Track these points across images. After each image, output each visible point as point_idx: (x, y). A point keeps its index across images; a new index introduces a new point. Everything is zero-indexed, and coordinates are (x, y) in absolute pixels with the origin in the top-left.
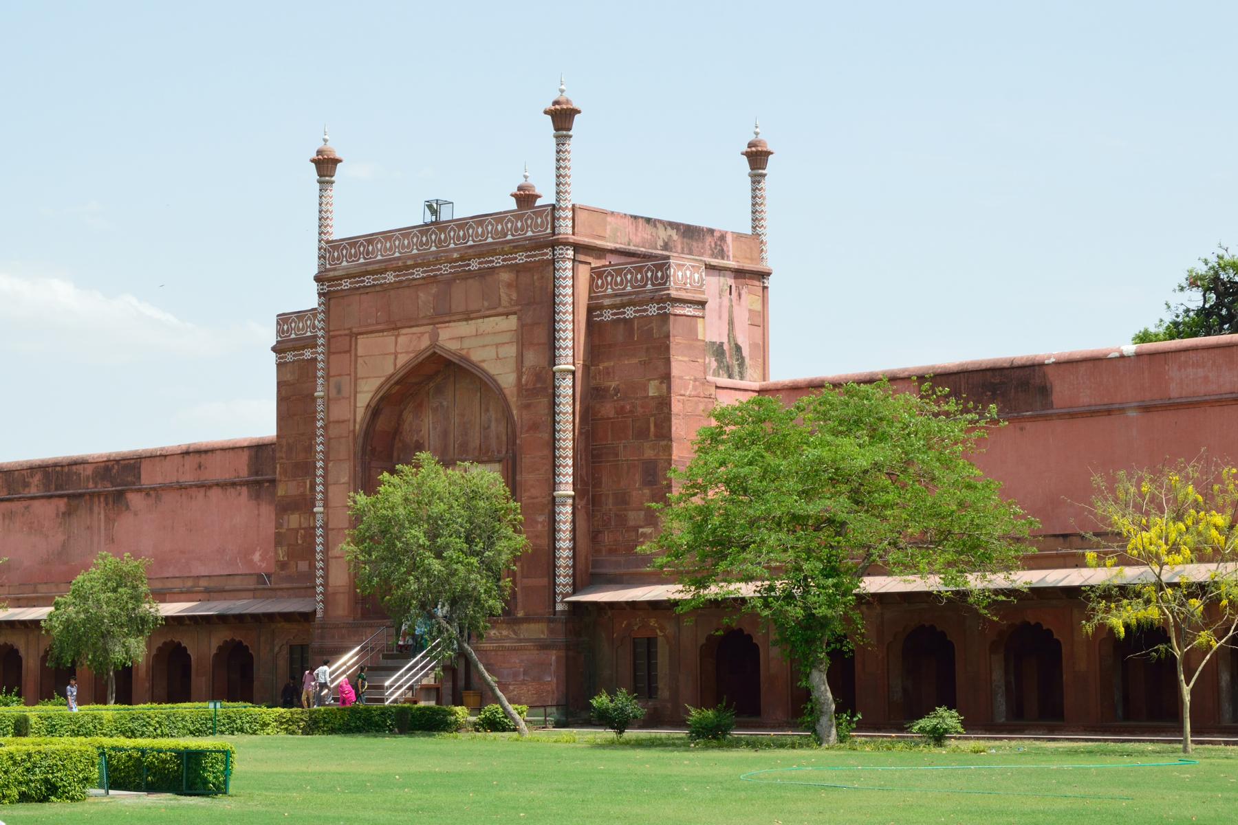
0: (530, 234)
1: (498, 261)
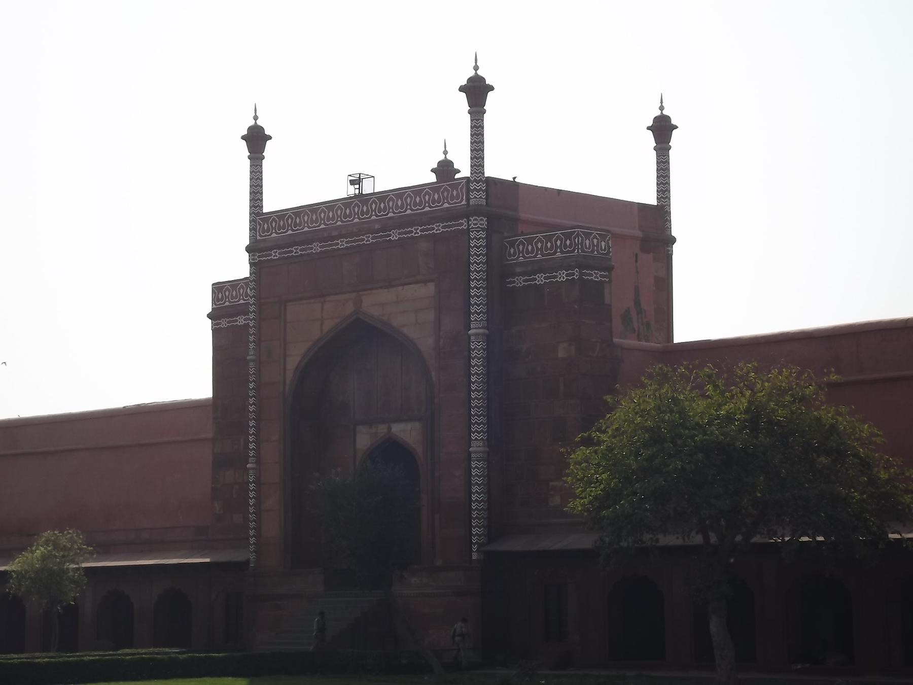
1: (417, 231)
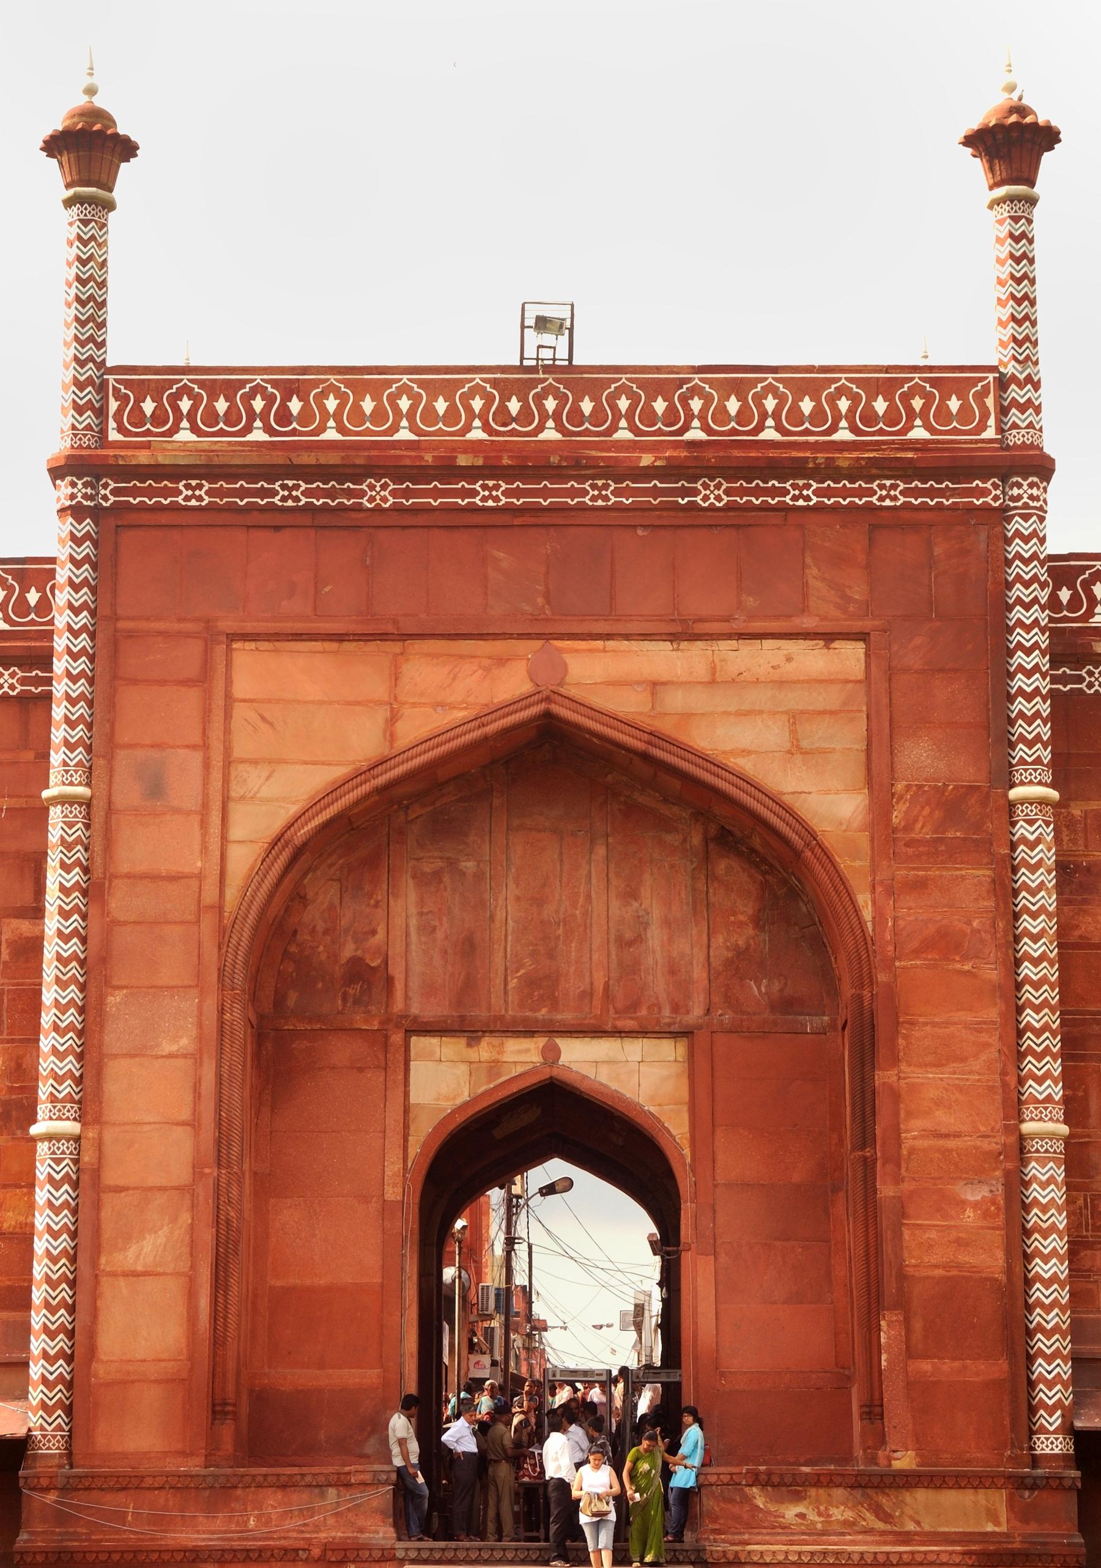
0: (919, 433)
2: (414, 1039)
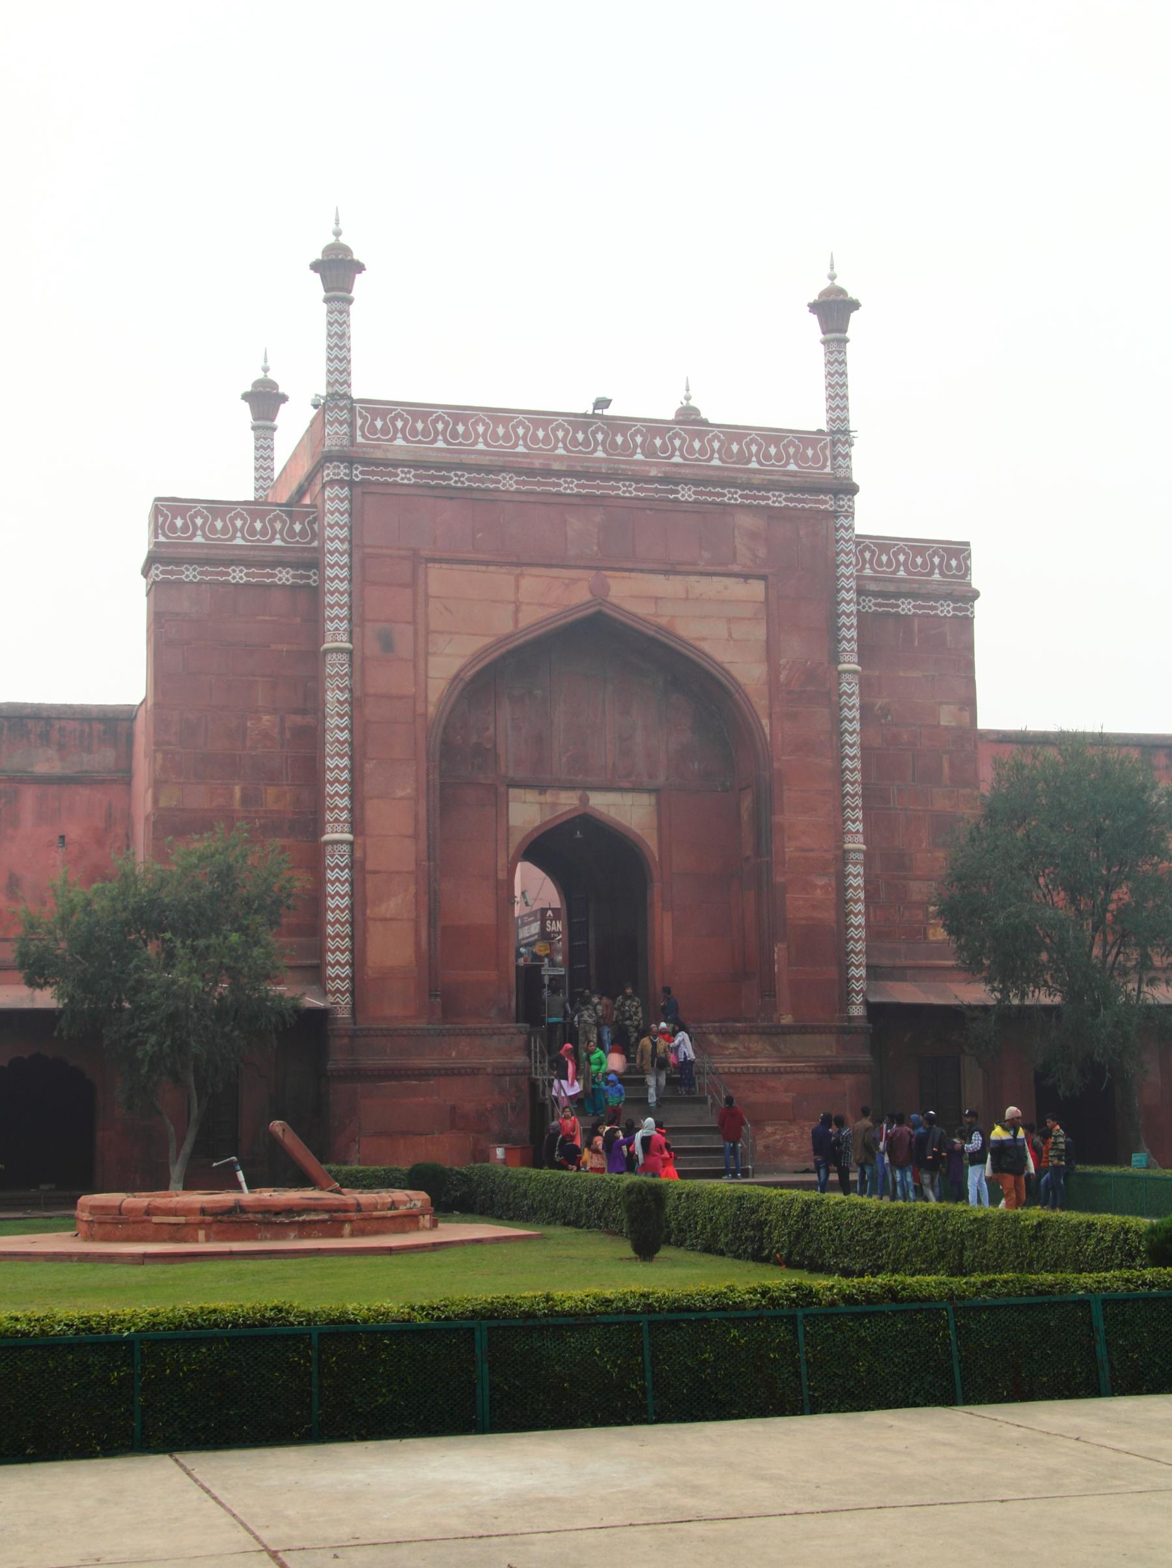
0: (792, 467)
2: (511, 791)
